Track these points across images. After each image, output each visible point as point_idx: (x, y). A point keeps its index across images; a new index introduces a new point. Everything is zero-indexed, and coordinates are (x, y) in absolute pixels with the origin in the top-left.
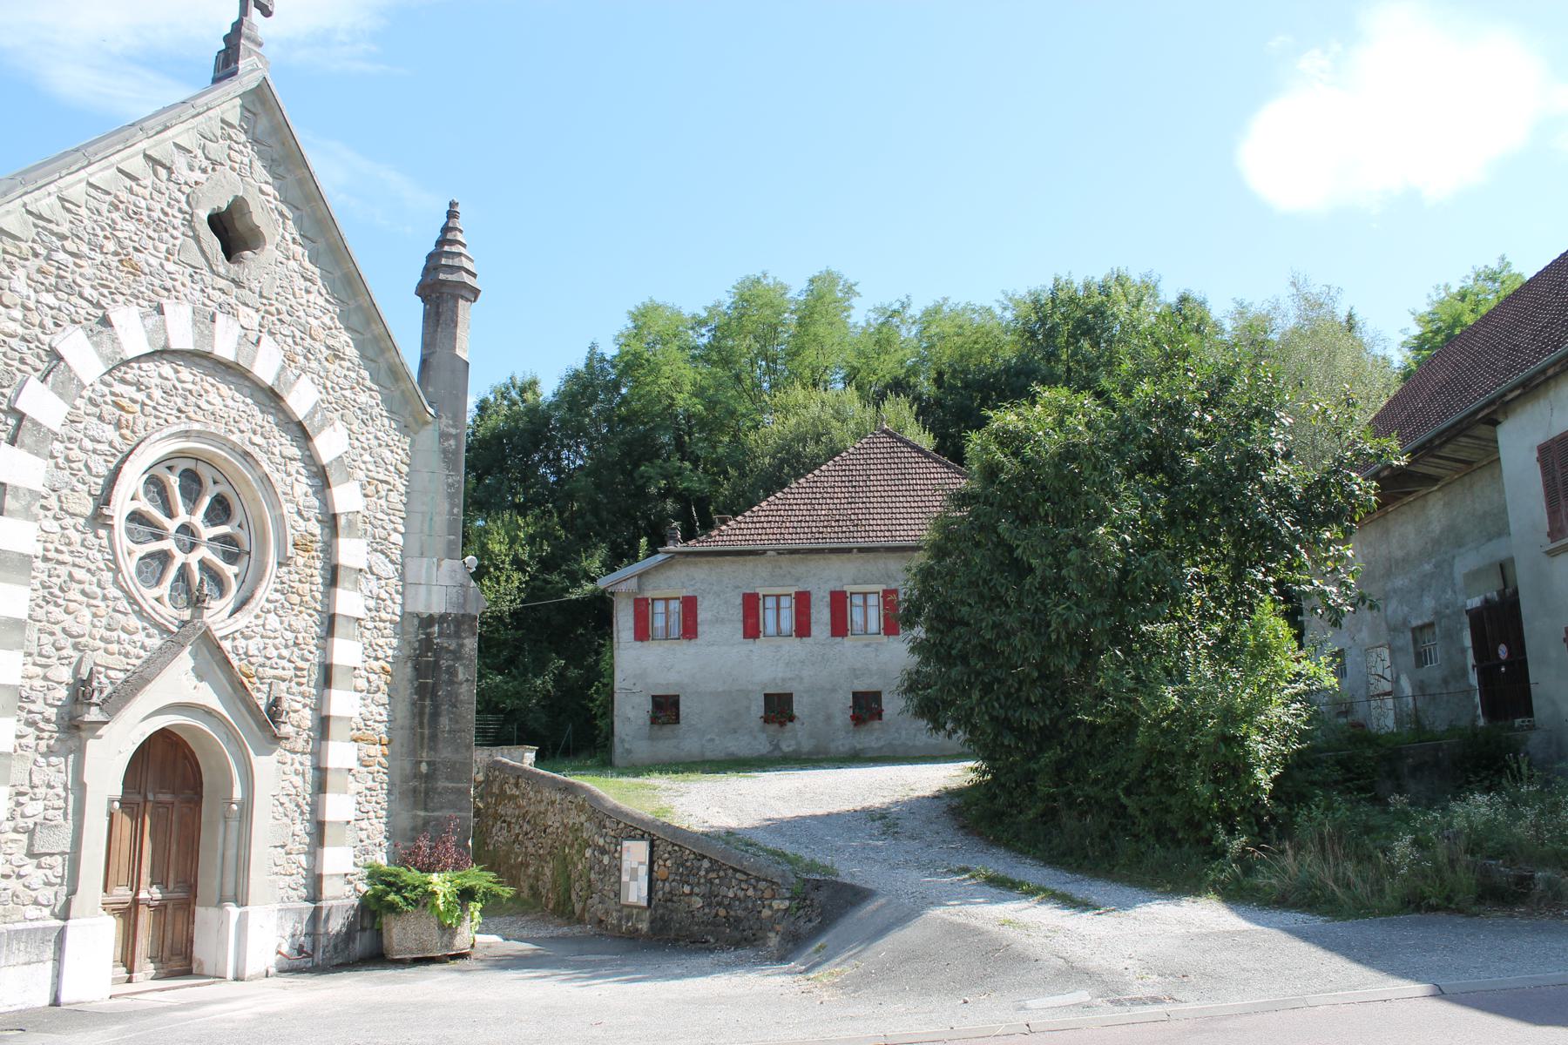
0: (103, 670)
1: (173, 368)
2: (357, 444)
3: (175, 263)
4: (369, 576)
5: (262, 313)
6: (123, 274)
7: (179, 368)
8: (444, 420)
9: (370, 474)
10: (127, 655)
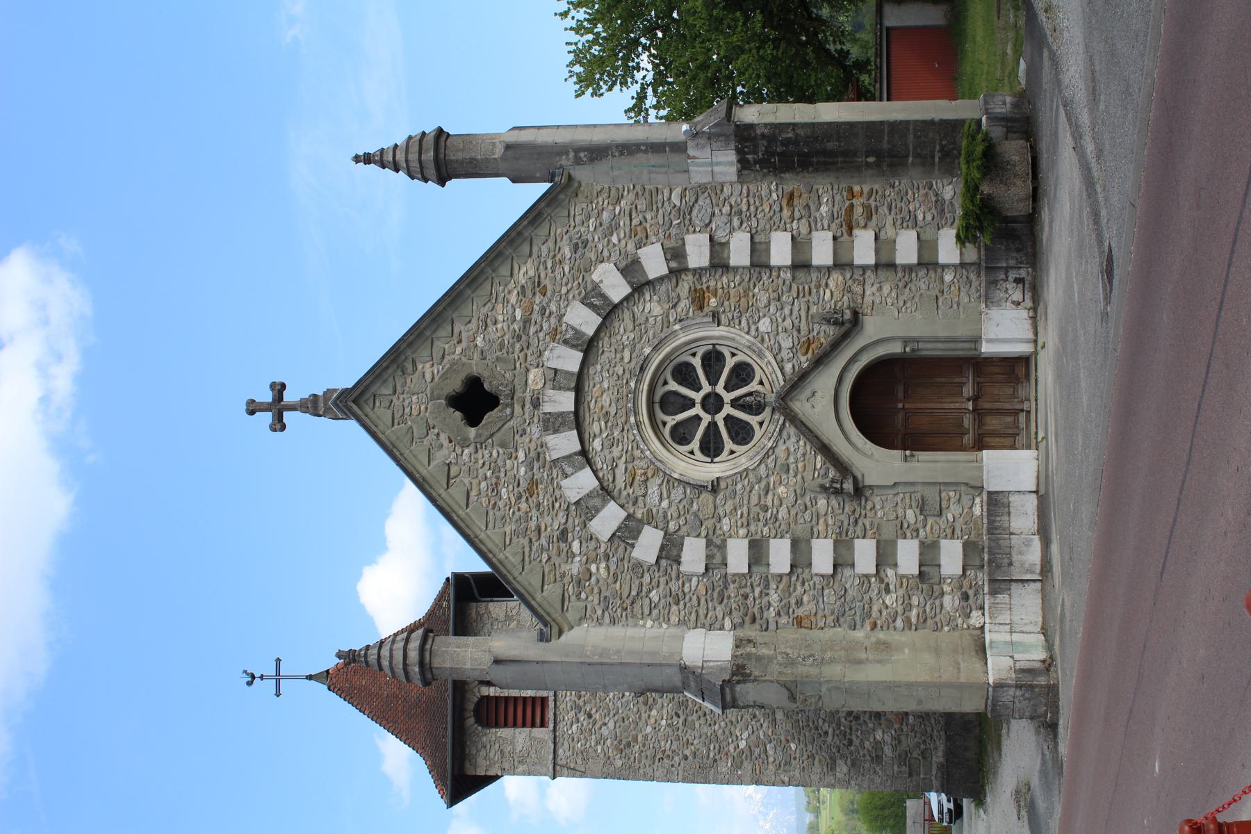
0: (817, 473)
1: (593, 440)
2: (606, 253)
3: (516, 451)
4: (714, 225)
5: (529, 367)
6: (541, 493)
7: (592, 435)
8: (564, 162)
9: (627, 235)
10: (804, 455)
